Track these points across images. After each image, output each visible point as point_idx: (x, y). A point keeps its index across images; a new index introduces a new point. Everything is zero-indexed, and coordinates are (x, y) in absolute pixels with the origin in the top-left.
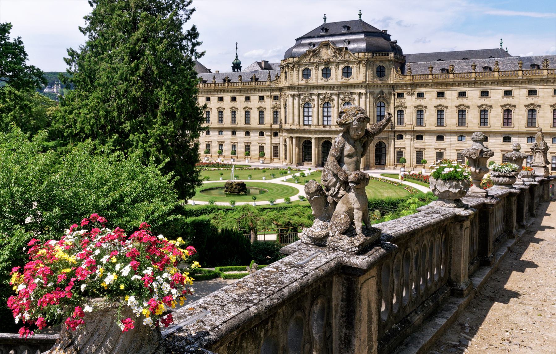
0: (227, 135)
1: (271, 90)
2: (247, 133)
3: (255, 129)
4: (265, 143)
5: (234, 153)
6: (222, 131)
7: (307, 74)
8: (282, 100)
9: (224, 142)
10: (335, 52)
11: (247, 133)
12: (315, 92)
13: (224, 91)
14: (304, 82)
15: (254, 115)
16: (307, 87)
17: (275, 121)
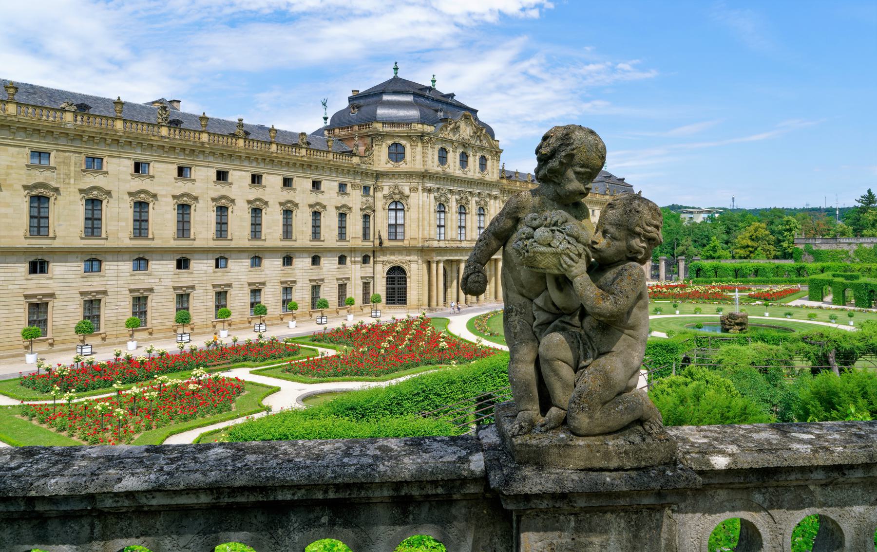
0: (272, 266)
1: (366, 174)
2: (316, 260)
3: (330, 251)
4: (348, 279)
5: (258, 309)
6: (260, 259)
7: (443, 158)
8: (379, 195)
9: (264, 284)
10: (475, 133)
11: (316, 260)
12: (456, 188)
13: (271, 161)
14: (440, 169)
15: (329, 221)
16: (448, 178)
17: (365, 236)
